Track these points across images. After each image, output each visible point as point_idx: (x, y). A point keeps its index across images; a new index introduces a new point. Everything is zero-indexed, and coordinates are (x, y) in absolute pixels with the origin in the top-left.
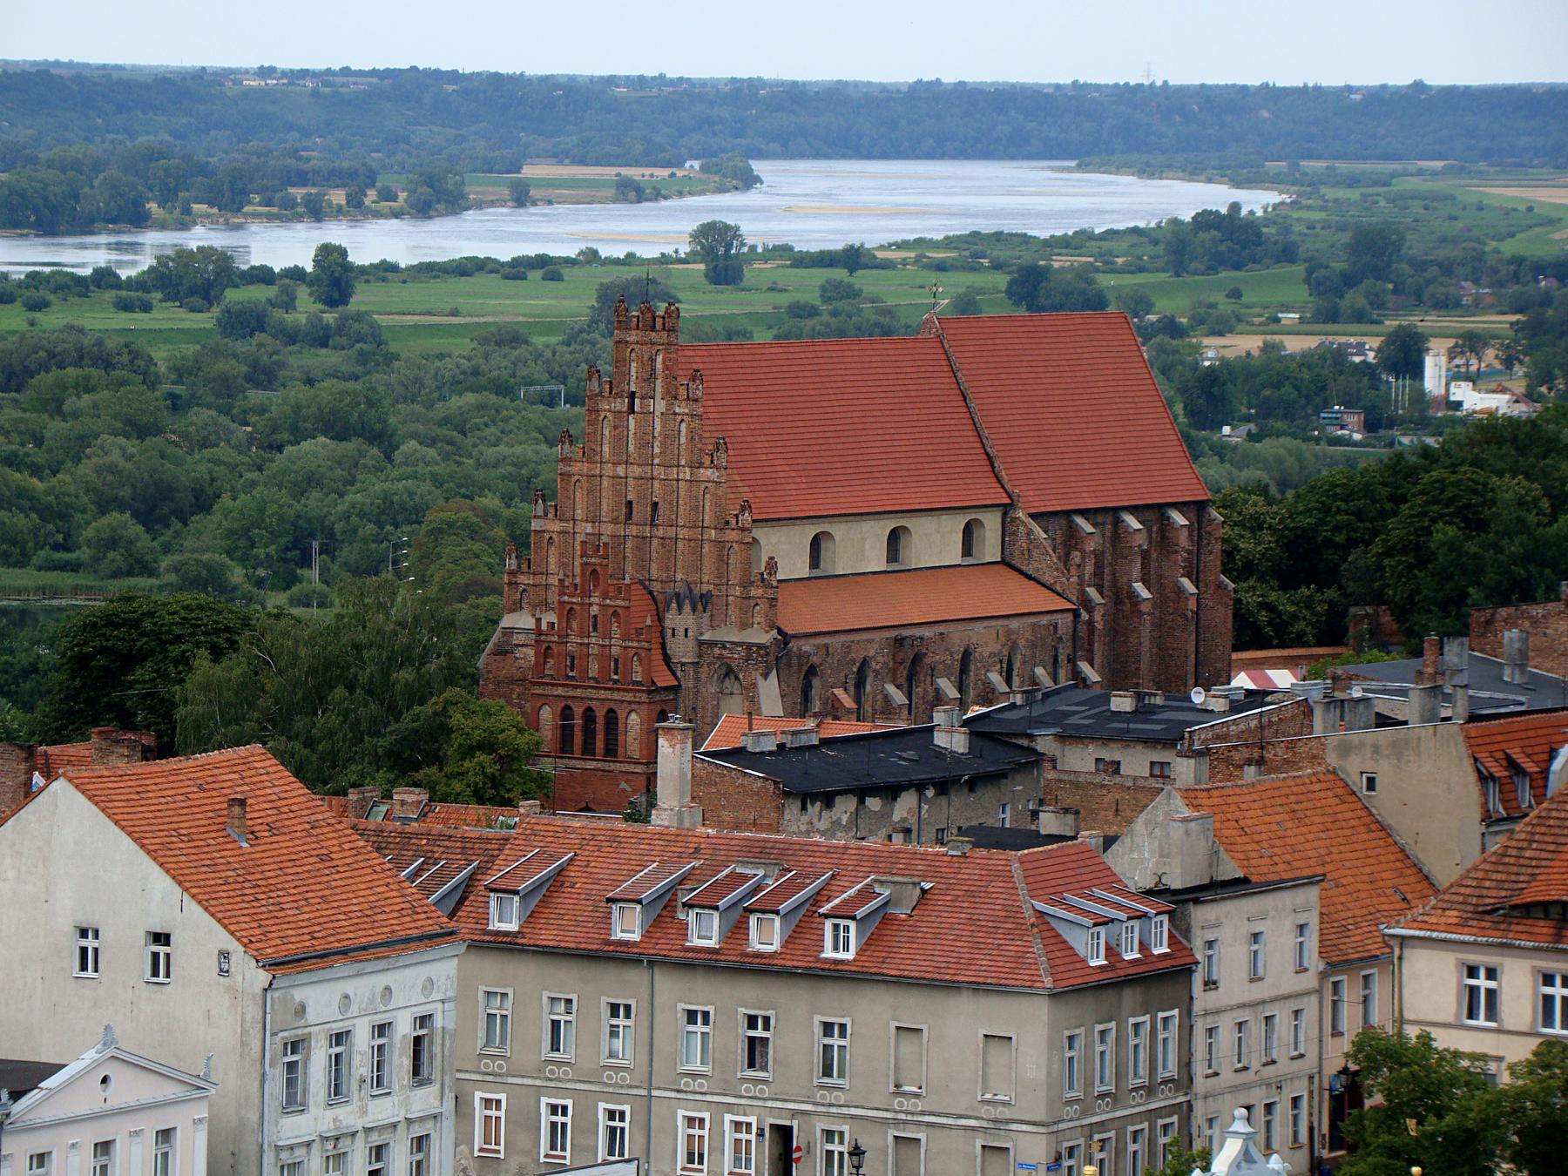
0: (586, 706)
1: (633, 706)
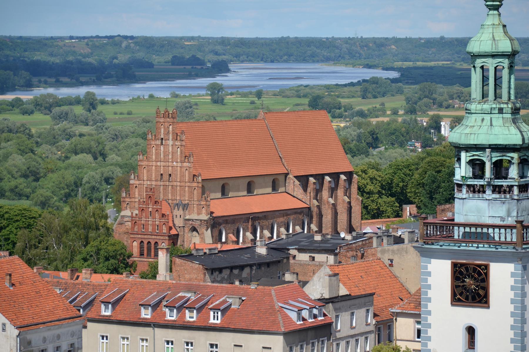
0: (148, 241)
1: (163, 241)
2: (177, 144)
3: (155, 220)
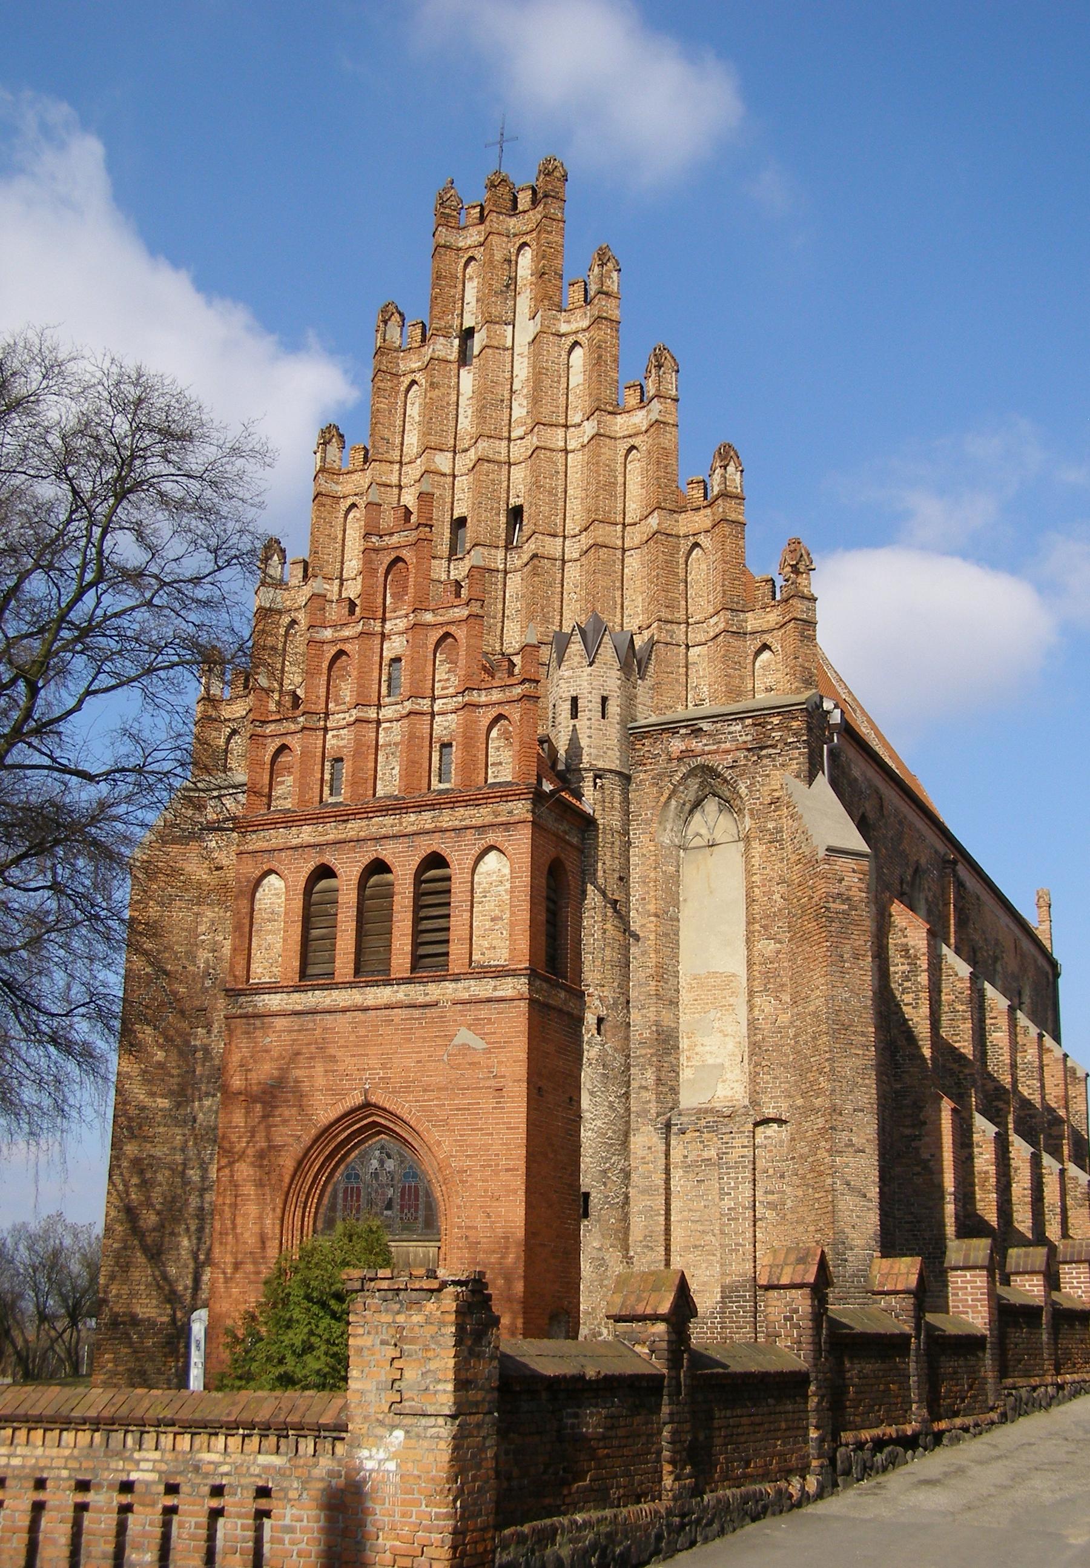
0: (372, 856)
1: (491, 838)
2: (564, 328)
3: (425, 704)
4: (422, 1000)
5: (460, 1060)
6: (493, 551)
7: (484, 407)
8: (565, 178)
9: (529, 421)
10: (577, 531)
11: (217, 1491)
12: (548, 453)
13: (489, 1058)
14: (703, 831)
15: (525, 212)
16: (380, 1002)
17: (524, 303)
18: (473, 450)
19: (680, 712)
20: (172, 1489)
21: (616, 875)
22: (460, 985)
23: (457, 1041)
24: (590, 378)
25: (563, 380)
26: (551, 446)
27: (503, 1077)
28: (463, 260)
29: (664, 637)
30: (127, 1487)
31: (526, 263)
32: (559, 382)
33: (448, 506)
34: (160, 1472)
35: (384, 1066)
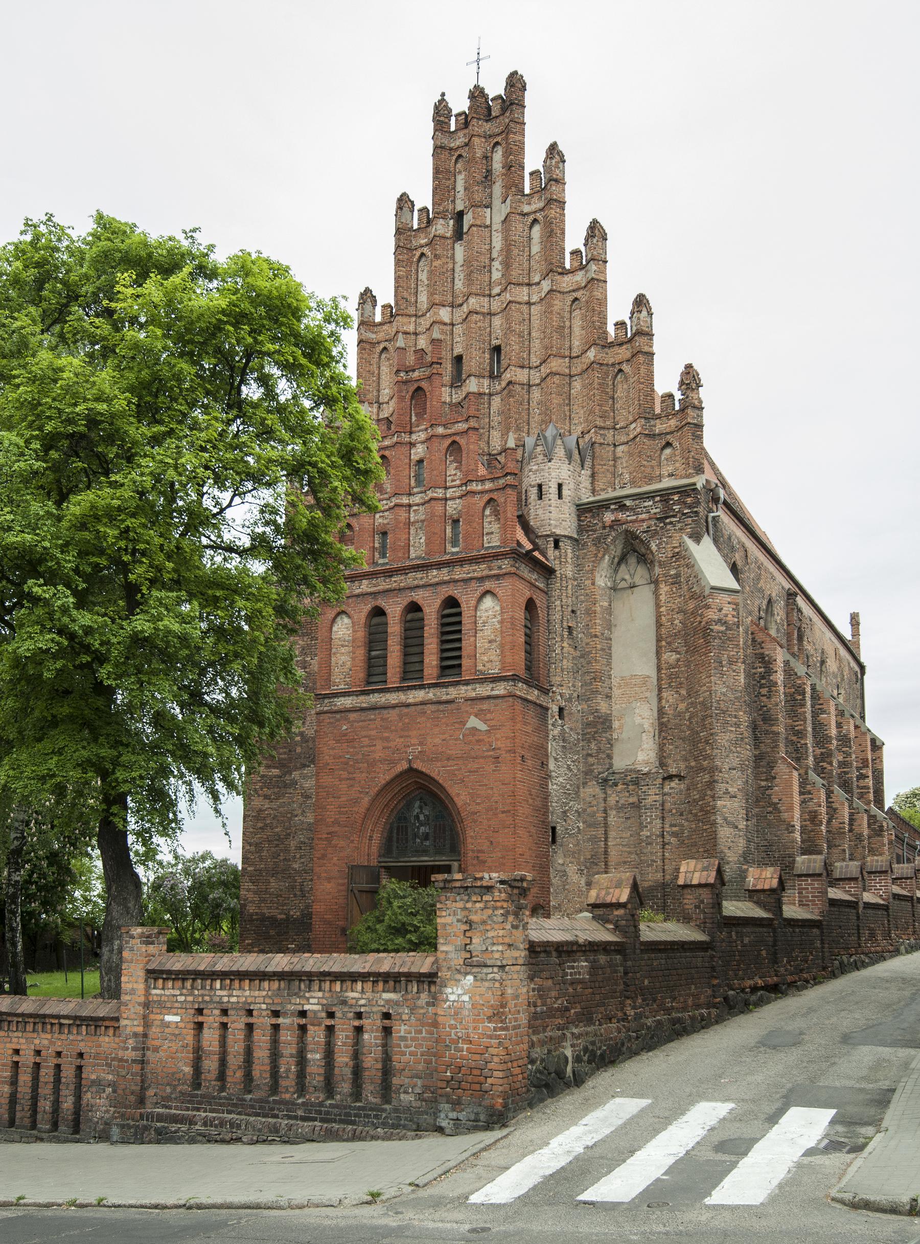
0: (405, 602)
2: (526, 209)
4: (444, 698)
5: (471, 738)
6: (481, 380)
7: (472, 272)
8: (524, 88)
9: (503, 282)
10: (538, 363)
11: (359, 1015)
12: (518, 306)
13: (489, 737)
14: (627, 577)
15: (497, 117)
16: (417, 700)
17: (498, 190)
18: (465, 305)
19: (611, 494)
20: (331, 1015)
21: (570, 609)
22: (469, 687)
23: (469, 725)
24: (546, 247)
25: (527, 249)
26: (520, 300)
27: (499, 749)
28: (454, 158)
29: (599, 439)
30: (303, 1014)
31: (498, 157)
32: (523, 251)
33: (449, 348)
34: (323, 1005)
35: (421, 744)
